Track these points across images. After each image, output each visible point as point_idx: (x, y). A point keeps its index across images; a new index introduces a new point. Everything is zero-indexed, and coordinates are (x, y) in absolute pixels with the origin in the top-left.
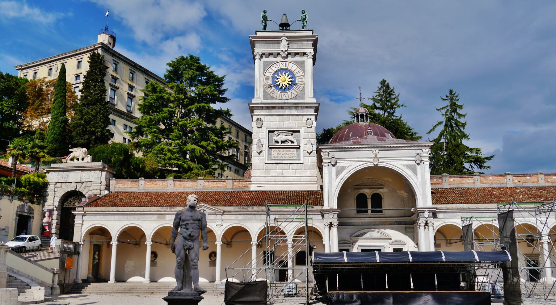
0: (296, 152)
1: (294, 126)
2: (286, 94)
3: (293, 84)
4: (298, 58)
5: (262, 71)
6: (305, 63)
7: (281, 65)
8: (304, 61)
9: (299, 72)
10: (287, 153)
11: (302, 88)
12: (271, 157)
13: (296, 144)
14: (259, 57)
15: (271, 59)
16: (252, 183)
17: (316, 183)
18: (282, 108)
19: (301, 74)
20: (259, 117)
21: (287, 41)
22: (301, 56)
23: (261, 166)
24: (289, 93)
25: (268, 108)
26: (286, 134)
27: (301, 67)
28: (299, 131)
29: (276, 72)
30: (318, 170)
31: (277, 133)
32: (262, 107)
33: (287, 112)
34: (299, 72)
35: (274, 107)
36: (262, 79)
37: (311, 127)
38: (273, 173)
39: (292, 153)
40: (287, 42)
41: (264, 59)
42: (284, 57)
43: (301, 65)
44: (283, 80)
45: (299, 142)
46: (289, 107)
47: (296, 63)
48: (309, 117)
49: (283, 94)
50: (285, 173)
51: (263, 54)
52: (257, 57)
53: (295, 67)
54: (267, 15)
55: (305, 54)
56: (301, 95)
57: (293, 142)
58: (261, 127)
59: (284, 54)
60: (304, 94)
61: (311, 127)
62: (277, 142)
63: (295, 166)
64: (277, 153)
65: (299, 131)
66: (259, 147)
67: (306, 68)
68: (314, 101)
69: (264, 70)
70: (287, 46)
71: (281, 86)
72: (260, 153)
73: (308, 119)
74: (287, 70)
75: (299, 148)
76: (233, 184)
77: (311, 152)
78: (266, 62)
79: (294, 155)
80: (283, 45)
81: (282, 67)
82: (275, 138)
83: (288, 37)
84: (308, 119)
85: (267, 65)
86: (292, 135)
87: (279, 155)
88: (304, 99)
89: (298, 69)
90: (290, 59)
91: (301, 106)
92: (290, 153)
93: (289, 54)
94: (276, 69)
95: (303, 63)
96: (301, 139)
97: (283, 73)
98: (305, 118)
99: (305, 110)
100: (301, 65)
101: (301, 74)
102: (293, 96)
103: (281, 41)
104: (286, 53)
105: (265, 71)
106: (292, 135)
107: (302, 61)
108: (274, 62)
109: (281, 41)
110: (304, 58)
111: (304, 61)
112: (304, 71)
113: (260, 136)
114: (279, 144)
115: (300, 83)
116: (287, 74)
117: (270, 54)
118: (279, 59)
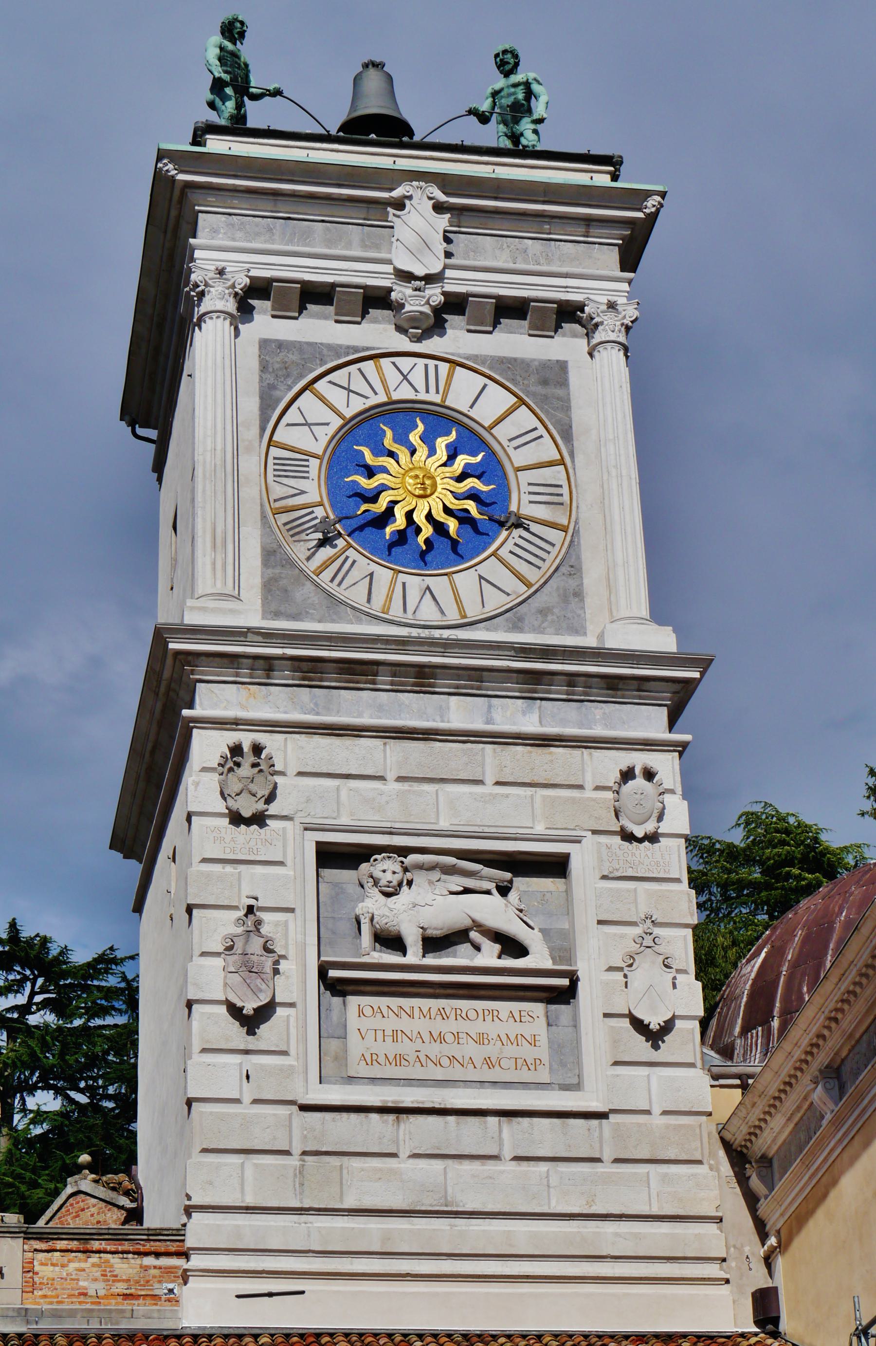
0: (539, 1027)
1: (523, 819)
2: (440, 585)
3: (482, 521)
5: (251, 405)
7: (393, 377)
8: (562, 366)
10: (477, 1027)
12: (342, 1058)
13: (539, 957)
14: (231, 306)
16: (197, 1261)
17: (713, 1270)
18: (422, 678)
19: (547, 450)
20: (246, 739)
21: (439, 208)
23: (270, 1125)
24: (466, 581)
25: (310, 672)
26: (457, 882)
27: (544, 400)
28: (556, 866)
29: (364, 426)
30: (726, 1168)
31: (386, 869)
32: (268, 664)
33: (459, 712)
35: (357, 673)
37: (653, 838)
38: (364, 1185)
39: (513, 1029)
40: (443, 221)
41: (265, 324)
42: (415, 320)
44: (421, 482)
45: (563, 948)
46: (474, 681)
48: (639, 759)
49: (414, 583)
50: (467, 1185)
52: (218, 300)
53: (496, 400)
54: (247, 51)
55: (568, 313)
57: (512, 947)
58: (259, 819)
60: (579, 594)
61: (653, 838)
62: (392, 941)
63: (545, 1136)
64: (390, 1024)
65: (556, 866)
66: (250, 969)
67: (581, 415)
68: (663, 640)
69: (267, 403)
70: (440, 247)
71: (400, 522)
72: (252, 1021)
73: (627, 775)
74: (439, 418)
75: (564, 995)
76: (28, 1269)
77: (667, 1027)
79: (526, 1051)
80: (417, 234)
81: (404, 393)
82: (373, 905)
83: (444, 181)
84: (627, 775)
86: (504, 890)
87: (406, 1047)
88: (579, 630)
89: (524, 419)
90: (457, 339)
91: (571, 679)
92: (492, 1028)
93: (455, 304)
94: (358, 405)
95: (556, 374)
96: (585, 916)
97: (414, 437)
98: (611, 763)
99: (598, 711)
101: (547, 450)
104: (435, 294)
105: (271, 408)
106: (504, 890)
108: (336, 350)
109: (399, 205)
110: (568, 346)
111: (562, 366)
112: (567, 434)
113: (252, 883)
114: (414, 956)
115: (541, 512)
116: (441, 443)
117: (314, 295)
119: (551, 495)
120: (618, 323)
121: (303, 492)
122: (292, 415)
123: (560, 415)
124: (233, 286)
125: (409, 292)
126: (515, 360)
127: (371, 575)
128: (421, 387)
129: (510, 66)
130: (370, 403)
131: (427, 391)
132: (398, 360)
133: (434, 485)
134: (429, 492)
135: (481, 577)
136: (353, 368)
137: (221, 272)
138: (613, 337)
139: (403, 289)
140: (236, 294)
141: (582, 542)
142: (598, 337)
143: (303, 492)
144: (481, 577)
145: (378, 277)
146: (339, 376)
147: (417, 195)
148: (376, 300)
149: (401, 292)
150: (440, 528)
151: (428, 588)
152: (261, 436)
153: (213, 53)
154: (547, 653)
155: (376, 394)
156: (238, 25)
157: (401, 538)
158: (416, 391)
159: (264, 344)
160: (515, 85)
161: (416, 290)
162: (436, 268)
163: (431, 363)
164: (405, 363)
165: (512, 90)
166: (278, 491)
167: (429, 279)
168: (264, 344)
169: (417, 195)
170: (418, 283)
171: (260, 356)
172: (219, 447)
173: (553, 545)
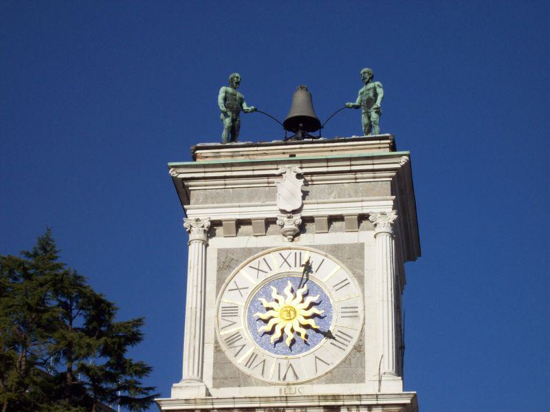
4: (340, 236)
6: (367, 252)
8: (362, 245)
9: (344, 284)
11: (354, 342)
14: (202, 236)
15: (244, 240)
21: (299, 176)
22: (350, 229)
34: (344, 284)
36: (211, 313)
40: (301, 182)
43: (353, 257)
47: (335, 251)
51: (216, 224)
52: (196, 235)
55: (363, 218)
56: (352, 366)
59: (291, 224)
71: (277, 335)
78: (227, 251)
80: (288, 190)
85: (228, 263)
94: (263, 277)
95: (359, 250)
100: (353, 257)
102: (323, 369)
103: (280, 175)
104: (297, 219)
107: (352, 246)
110: (363, 236)
111: (362, 245)
118: (273, 239)
119: (351, 312)
120: (386, 222)
121: (235, 323)
122: (232, 285)
123: (359, 271)
124: (203, 227)
125: (285, 219)
126: (339, 245)
127: (265, 361)
128: (292, 264)
129: (367, 80)
130: (268, 275)
131: (296, 266)
132: (282, 252)
133: (295, 313)
134: (292, 317)
135: (316, 357)
136: (261, 259)
137: (198, 220)
138: (384, 229)
139: (282, 218)
140: (205, 231)
141: (366, 335)
142: (378, 230)
143: (235, 323)
144: (316, 357)
145: (271, 212)
146: (253, 264)
147: (288, 171)
148: (269, 222)
149: (283, 218)
150: (307, 327)
151: (291, 365)
152: (217, 297)
153: (221, 95)
154: (335, 397)
155: (271, 270)
156: (235, 79)
157: (281, 340)
158: (290, 266)
159: (220, 251)
160: (368, 90)
161: (288, 218)
162: (297, 207)
163: (298, 252)
164: (285, 253)
165: (367, 92)
166: (223, 323)
167: (294, 212)
168: (220, 251)
169: (288, 171)
170: (289, 215)
171: (218, 258)
172: (194, 306)
173: (351, 338)
